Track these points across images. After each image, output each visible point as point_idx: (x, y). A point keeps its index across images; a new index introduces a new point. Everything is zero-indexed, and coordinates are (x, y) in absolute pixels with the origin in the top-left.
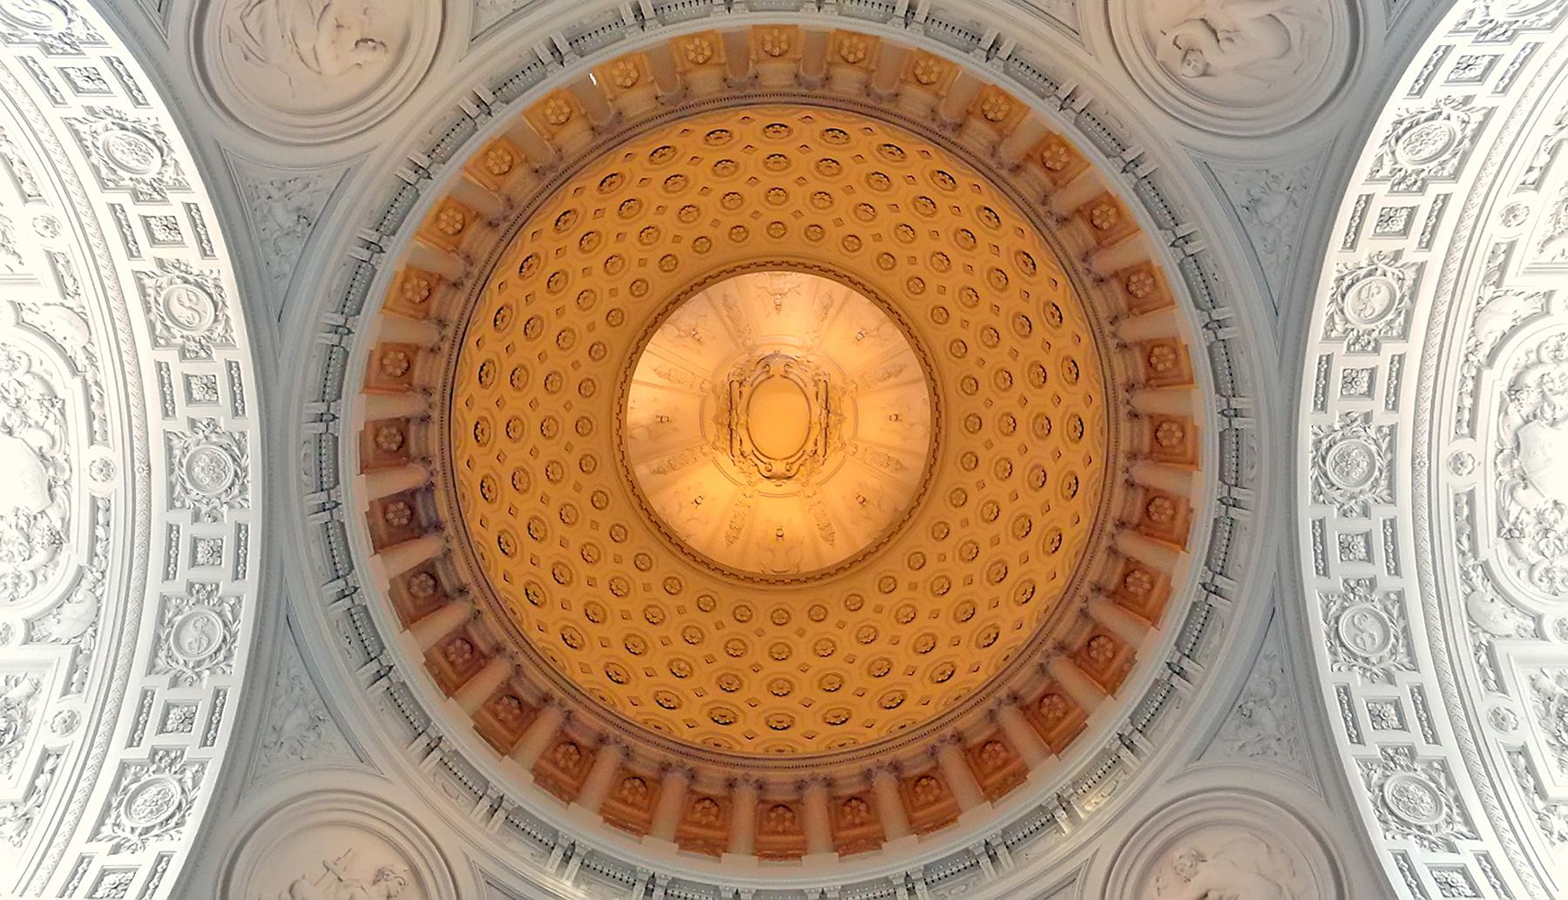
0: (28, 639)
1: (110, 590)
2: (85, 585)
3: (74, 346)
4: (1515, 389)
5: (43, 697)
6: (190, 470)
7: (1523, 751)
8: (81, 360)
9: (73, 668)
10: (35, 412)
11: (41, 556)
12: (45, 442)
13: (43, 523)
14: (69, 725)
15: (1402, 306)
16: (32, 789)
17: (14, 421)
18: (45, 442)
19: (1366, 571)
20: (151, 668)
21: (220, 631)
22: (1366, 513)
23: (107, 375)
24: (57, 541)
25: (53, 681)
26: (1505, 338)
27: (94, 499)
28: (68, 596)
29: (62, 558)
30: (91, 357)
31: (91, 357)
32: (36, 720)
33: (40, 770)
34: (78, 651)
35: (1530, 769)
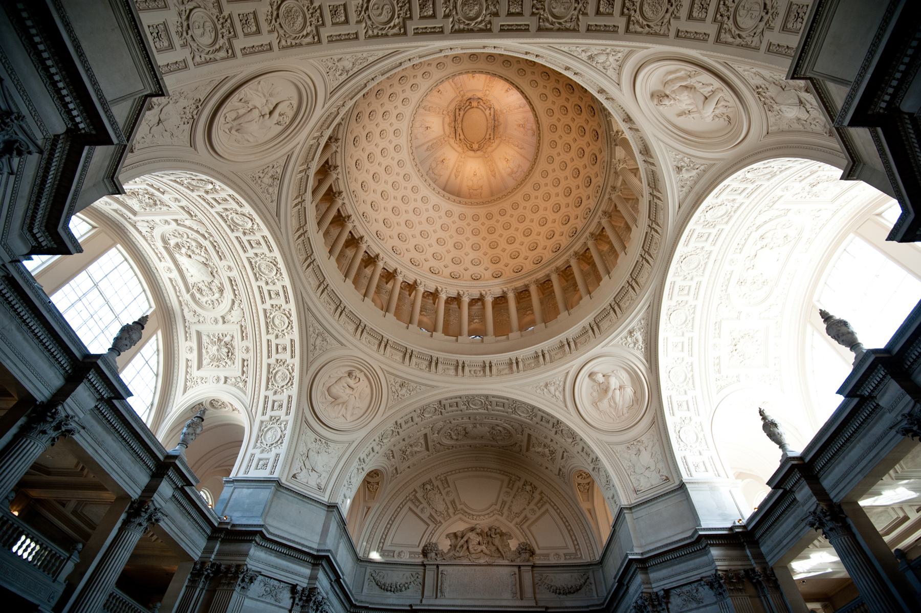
0: (224, 322)
1: (245, 305)
2: (236, 305)
3: (203, 231)
4: (762, 238)
5: (236, 339)
6: (260, 269)
7: (719, 358)
8: (207, 235)
9: (242, 332)
10: (197, 251)
11: (217, 295)
12: (204, 260)
13: (213, 284)
14: (247, 350)
15: (728, 216)
16: (243, 372)
17: (189, 253)
18: (204, 260)
19: (685, 298)
20: (268, 332)
21: (287, 321)
22: (692, 279)
23: (217, 238)
24: (221, 291)
25: (238, 336)
26: (765, 222)
27: (229, 278)
28: (232, 308)
29: (224, 295)
30: (209, 234)
31: (209, 234)
32: (236, 347)
33: (243, 366)
34: (242, 326)
35: (719, 364)
